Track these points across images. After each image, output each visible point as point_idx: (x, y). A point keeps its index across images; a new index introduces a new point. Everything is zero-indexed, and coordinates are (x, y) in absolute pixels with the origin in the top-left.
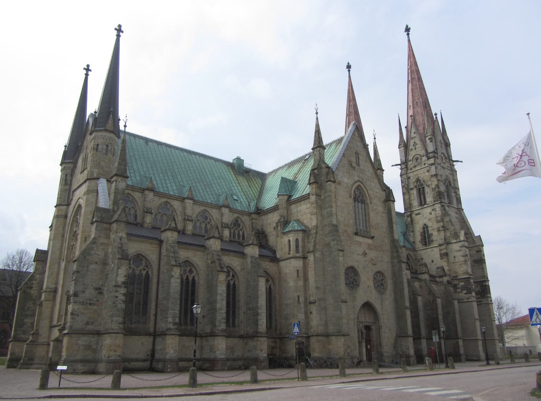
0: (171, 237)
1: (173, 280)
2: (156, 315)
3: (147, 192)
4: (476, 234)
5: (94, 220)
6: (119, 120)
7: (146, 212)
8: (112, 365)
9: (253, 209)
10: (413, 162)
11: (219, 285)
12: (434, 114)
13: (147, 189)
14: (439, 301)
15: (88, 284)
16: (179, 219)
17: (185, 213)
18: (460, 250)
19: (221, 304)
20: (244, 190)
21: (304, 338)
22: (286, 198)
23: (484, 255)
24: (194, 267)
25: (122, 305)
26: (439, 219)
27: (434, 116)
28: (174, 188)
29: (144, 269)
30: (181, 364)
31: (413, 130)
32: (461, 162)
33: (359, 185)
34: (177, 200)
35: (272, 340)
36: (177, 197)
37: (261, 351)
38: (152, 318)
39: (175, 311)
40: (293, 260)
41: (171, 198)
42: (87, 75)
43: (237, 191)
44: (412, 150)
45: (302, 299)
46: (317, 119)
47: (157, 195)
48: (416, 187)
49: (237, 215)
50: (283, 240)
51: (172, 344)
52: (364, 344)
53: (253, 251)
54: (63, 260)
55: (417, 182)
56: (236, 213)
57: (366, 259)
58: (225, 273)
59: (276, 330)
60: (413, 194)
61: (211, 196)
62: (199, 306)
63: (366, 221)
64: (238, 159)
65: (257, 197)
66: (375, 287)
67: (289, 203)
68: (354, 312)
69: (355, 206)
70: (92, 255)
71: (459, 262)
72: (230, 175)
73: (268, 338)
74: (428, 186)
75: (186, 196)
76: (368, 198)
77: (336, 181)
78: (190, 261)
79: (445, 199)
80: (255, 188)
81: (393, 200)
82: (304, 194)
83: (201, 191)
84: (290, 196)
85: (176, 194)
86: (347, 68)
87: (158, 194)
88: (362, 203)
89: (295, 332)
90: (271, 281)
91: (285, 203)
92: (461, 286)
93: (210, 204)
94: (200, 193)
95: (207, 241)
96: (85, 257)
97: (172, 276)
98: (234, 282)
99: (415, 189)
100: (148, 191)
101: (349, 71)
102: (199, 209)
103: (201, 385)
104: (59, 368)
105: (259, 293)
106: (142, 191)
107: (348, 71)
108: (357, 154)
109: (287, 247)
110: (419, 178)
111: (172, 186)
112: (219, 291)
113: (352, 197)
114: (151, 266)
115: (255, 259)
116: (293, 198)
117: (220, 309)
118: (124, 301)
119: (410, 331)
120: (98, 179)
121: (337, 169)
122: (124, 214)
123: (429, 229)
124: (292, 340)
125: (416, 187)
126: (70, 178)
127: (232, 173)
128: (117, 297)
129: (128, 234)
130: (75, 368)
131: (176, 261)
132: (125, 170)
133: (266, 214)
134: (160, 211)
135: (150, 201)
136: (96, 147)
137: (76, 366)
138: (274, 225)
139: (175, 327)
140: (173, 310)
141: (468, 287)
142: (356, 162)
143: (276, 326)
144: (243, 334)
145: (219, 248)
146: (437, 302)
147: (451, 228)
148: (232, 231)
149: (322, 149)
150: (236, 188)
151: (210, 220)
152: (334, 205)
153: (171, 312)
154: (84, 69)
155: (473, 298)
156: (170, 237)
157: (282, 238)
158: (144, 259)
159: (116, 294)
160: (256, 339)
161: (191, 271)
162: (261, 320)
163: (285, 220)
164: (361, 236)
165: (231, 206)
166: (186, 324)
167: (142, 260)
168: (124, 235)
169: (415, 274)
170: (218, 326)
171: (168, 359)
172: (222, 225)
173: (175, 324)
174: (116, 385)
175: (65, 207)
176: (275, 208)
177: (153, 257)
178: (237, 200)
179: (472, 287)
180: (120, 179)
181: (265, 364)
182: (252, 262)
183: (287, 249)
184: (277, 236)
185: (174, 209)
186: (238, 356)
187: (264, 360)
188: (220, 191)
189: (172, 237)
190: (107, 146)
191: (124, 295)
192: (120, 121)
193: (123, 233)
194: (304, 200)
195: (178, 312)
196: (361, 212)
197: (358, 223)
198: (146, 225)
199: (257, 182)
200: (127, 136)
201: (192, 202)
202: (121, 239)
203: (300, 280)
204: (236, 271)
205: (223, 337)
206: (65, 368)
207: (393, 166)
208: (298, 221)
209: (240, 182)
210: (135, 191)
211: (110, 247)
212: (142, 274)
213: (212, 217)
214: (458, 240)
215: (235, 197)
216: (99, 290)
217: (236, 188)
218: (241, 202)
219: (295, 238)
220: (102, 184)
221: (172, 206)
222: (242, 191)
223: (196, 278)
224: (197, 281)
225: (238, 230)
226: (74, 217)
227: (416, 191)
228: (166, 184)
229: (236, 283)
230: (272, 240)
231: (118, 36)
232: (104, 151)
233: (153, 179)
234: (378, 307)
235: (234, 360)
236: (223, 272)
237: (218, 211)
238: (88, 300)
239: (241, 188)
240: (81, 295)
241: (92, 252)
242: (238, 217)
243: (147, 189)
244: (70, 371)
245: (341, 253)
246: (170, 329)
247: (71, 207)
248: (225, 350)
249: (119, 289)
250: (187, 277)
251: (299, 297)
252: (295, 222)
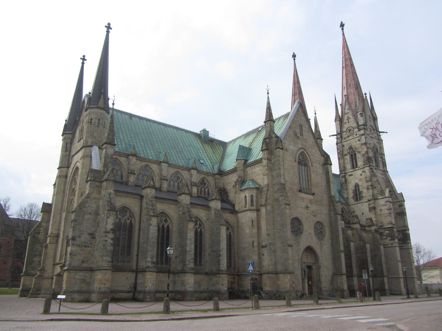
0: (150, 193)
1: (151, 228)
2: (138, 256)
3: (131, 157)
4: (399, 192)
5: (89, 179)
6: (109, 99)
7: (130, 173)
8: (102, 295)
9: (216, 171)
10: (346, 133)
11: (189, 232)
12: (364, 93)
13: (131, 155)
14: (368, 246)
15: (83, 230)
16: (157, 179)
17: (161, 174)
18: (386, 205)
19: (190, 247)
20: (209, 156)
21: (258, 275)
22: (243, 162)
23: (405, 209)
24: (169, 217)
25: (111, 247)
26: (368, 179)
27: (364, 96)
28: (153, 154)
29: (128, 219)
30: (158, 295)
31: (347, 107)
32: (387, 133)
33: (303, 152)
34: (154, 163)
35: (232, 276)
36: (155, 161)
37: (223, 285)
38: (135, 258)
39: (153, 253)
40: (249, 212)
41: (150, 162)
42: (83, 63)
43: (203, 156)
44: (345, 123)
45: (256, 244)
46: (268, 98)
47: (139, 159)
48: (349, 153)
49: (203, 176)
50: (240, 196)
51: (150, 279)
52: (306, 281)
53: (216, 205)
54: (64, 211)
55: (350, 149)
56: (202, 174)
57: (308, 211)
58: (193, 222)
59: (235, 269)
60: (347, 159)
61: (182, 161)
62: (172, 248)
63: (308, 181)
64: (204, 131)
65: (219, 161)
66: (315, 234)
67: (246, 166)
68: (298, 255)
69: (299, 169)
70: (87, 207)
71: (385, 214)
72: (197, 143)
73: (228, 274)
74: (359, 152)
75: (162, 160)
76: (310, 162)
77: (284, 148)
78: (165, 212)
79: (373, 163)
80: (218, 154)
81: (330, 163)
82: (257, 159)
83: (174, 156)
84: (246, 161)
85: (154, 159)
86: (293, 57)
87: (140, 158)
88: (305, 166)
89: (250, 270)
90: (230, 229)
91: (242, 166)
92: (386, 234)
93: (182, 167)
94: (173, 158)
95: (179, 196)
96: (81, 209)
97: (151, 225)
98: (201, 229)
99: (348, 155)
100: (131, 156)
101: (294, 59)
102: (172, 171)
103: (173, 312)
104: (59, 297)
105: (221, 238)
106: (127, 156)
107: (294, 59)
108: (301, 126)
109: (244, 201)
110: (352, 146)
111: (151, 153)
112: (189, 237)
113: (297, 161)
114: (134, 216)
115: (218, 211)
116: (248, 162)
117: (189, 251)
118: (112, 244)
119: (344, 270)
120: (91, 146)
121: (284, 138)
122: (112, 175)
123: (360, 187)
124: (248, 276)
125: (349, 153)
126: (69, 146)
127: (200, 142)
128: (106, 241)
129: (116, 191)
130: (72, 298)
131: (154, 212)
132: (113, 140)
133: (226, 175)
134: (141, 173)
135: (133, 165)
136: (90, 121)
137: (74, 295)
138: (234, 184)
139: (153, 265)
140: (152, 251)
141: (392, 235)
142: (300, 133)
143: (235, 265)
144: (208, 271)
145: (188, 202)
146: (367, 247)
147: (378, 187)
148: (199, 189)
149: (272, 122)
150: (202, 154)
151: (181, 180)
152: (282, 168)
153: (150, 253)
154: (81, 59)
155: (396, 244)
156: (149, 193)
157: (240, 194)
158: (128, 211)
159: (106, 239)
160: (218, 275)
161: (166, 221)
162: (223, 260)
163: (242, 179)
164: (304, 193)
165: (199, 169)
166: (162, 263)
167: (126, 211)
168: (112, 191)
169: (348, 224)
170: (188, 265)
171: (148, 291)
172: (191, 184)
173: (153, 263)
174: (105, 311)
175: (65, 169)
176: (234, 170)
177: (135, 209)
178: (204, 164)
179: (395, 235)
180: (109, 146)
181: (226, 296)
182: (215, 213)
183: (244, 203)
184: (236, 193)
185: (152, 170)
186: (204, 289)
187: (225, 292)
188: (189, 156)
189: (151, 193)
190: (99, 120)
191: (112, 239)
192: (109, 100)
193: (112, 190)
194: (257, 163)
195: (155, 253)
196: (304, 173)
197: (301, 183)
198: (130, 184)
199: (220, 149)
200: (115, 113)
201: (167, 165)
202: (110, 194)
203: (254, 228)
204: (202, 220)
205: (192, 274)
206: (64, 297)
207: (330, 136)
208: (253, 180)
209: (205, 149)
210: (122, 156)
211: (101, 201)
212: (126, 223)
213: (183, 177)
214: (384, 197)
215: (202, 162)
216: (92, 235)
217: (202, 154)
218: (207, 166)
219: (251, 194)
220: (95, 151)
221: (151, 169)
222: (208, 156)
223: (170, 226)
224: (171, 228)
225: (204, 188)
226: (73, 177)
227: (349, 156)
228: (146, 150)
229: (203, 230)
230: (231, 196)
231: (108, 32)
232: (97, 124)
233: (136, 146)
234: (318, 250)
235: (201, 292)
236: (192, 221)
237: (188, 172)
238: (83, 243)
239: (207, 154)
240: (78, 239)
241: (87, 205)
242: (204, 177)
243: (131, 155)
244: (69, 300)
245: (287, 207)
246: (149, 267)
247: (71, 169)
248: (193, 284)
249: (108, 234)
250: (163, 225)
251: (253, 242)
252: (250, 182)
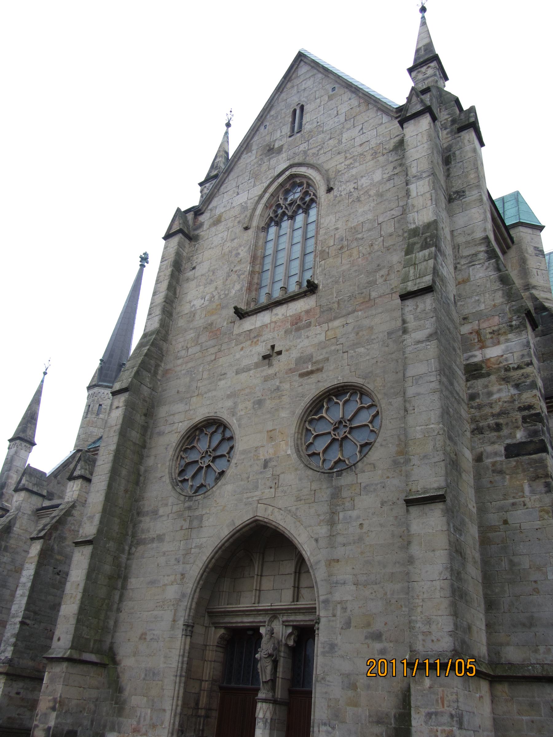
57: (271, 371)
231: (142, 266)
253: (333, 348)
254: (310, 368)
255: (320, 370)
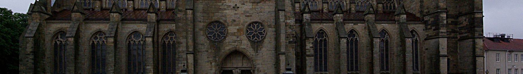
0: (74, 17)
57: (236, 12)
166: (352, 70)
253: (254, 11)
254: (248, 15)
255: (251, 16)
